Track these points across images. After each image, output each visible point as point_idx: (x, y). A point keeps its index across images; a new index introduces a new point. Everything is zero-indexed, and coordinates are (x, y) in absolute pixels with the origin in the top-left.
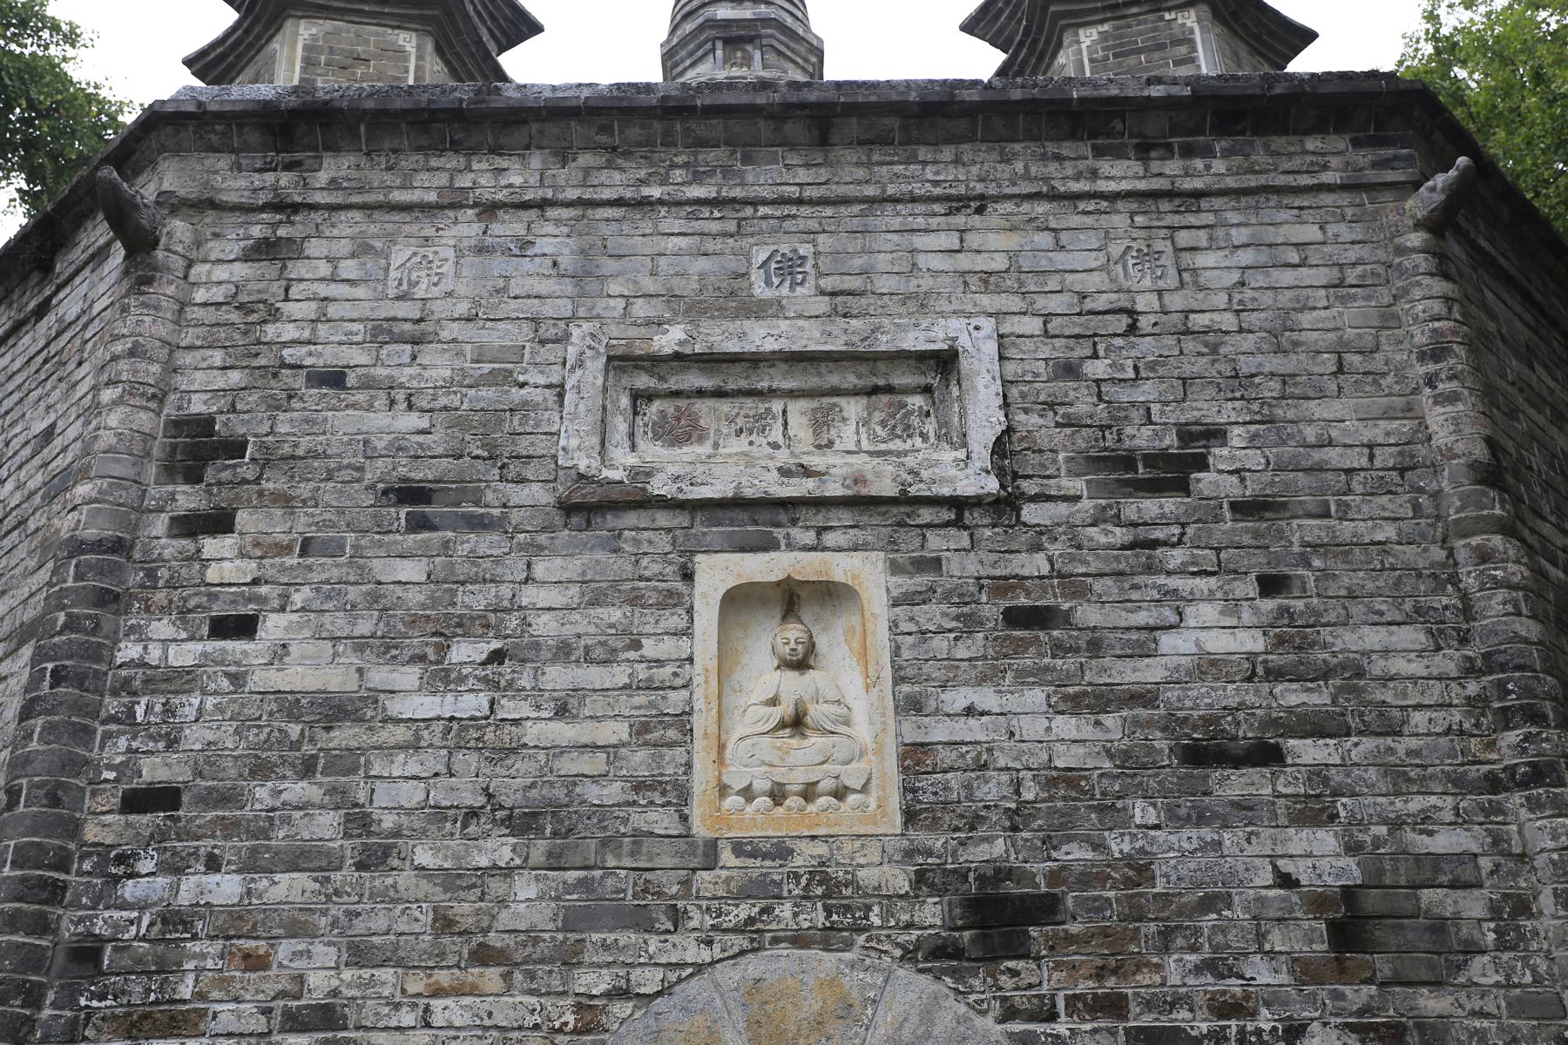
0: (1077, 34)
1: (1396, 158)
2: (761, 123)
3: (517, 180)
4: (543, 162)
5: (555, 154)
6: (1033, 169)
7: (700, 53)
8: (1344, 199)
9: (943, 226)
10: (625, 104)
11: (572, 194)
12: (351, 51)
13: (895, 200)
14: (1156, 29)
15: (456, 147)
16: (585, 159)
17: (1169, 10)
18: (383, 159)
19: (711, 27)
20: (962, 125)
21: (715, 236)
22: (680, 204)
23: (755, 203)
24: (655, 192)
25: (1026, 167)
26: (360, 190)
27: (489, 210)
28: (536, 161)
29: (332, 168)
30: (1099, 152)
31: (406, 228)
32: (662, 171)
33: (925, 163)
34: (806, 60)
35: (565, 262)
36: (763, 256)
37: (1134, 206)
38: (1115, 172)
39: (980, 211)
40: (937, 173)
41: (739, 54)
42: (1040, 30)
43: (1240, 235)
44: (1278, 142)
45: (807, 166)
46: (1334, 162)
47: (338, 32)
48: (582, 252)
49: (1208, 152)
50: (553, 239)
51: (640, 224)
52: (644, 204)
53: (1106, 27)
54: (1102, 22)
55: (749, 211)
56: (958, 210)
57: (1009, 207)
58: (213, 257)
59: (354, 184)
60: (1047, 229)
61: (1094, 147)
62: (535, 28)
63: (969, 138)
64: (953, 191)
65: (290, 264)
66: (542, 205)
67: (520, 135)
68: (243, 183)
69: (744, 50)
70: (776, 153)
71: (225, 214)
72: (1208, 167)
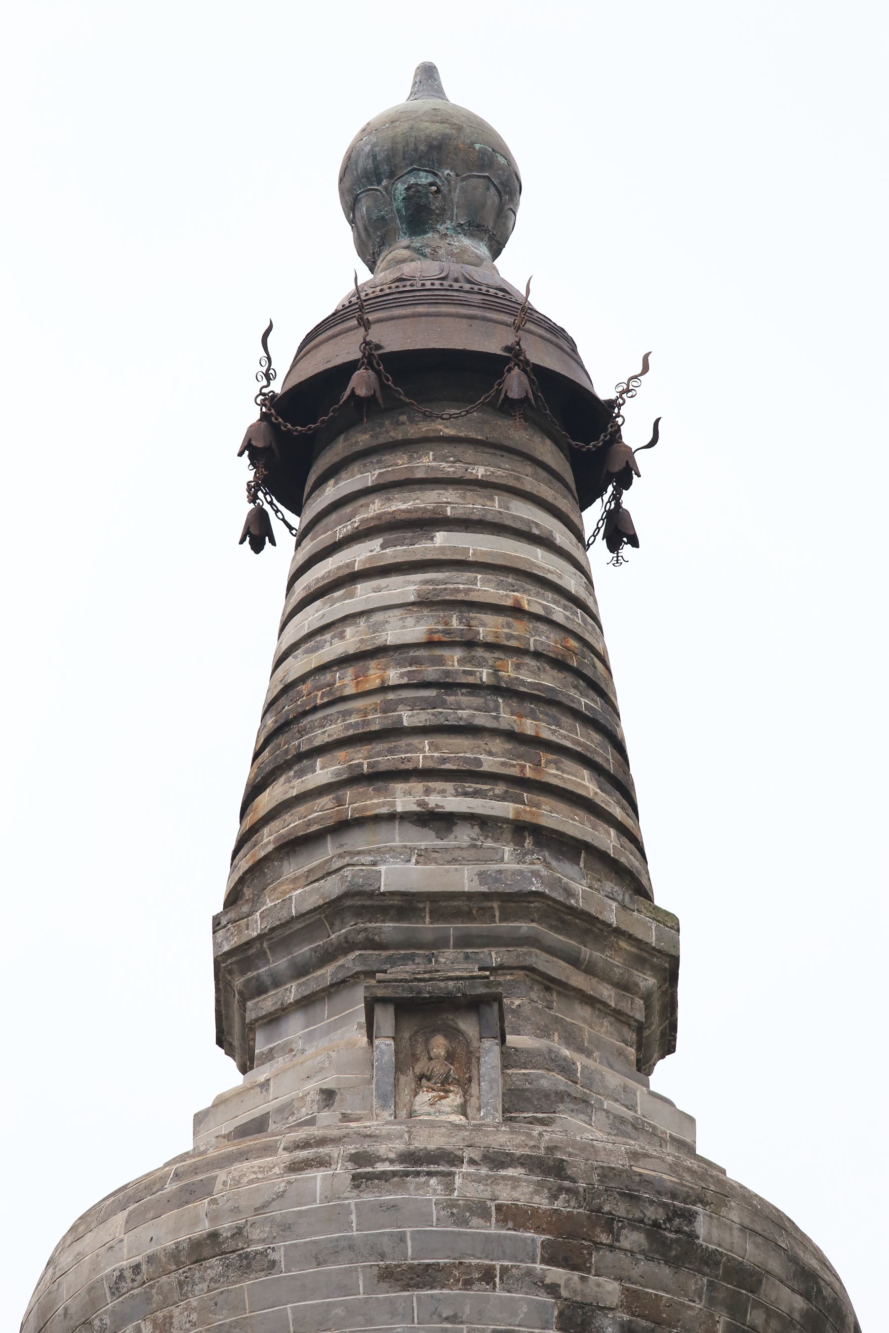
7: (327, 974)
19: (360, 912)
34: (625, 987)
41: (439, 1045)
69: (453, 1033)
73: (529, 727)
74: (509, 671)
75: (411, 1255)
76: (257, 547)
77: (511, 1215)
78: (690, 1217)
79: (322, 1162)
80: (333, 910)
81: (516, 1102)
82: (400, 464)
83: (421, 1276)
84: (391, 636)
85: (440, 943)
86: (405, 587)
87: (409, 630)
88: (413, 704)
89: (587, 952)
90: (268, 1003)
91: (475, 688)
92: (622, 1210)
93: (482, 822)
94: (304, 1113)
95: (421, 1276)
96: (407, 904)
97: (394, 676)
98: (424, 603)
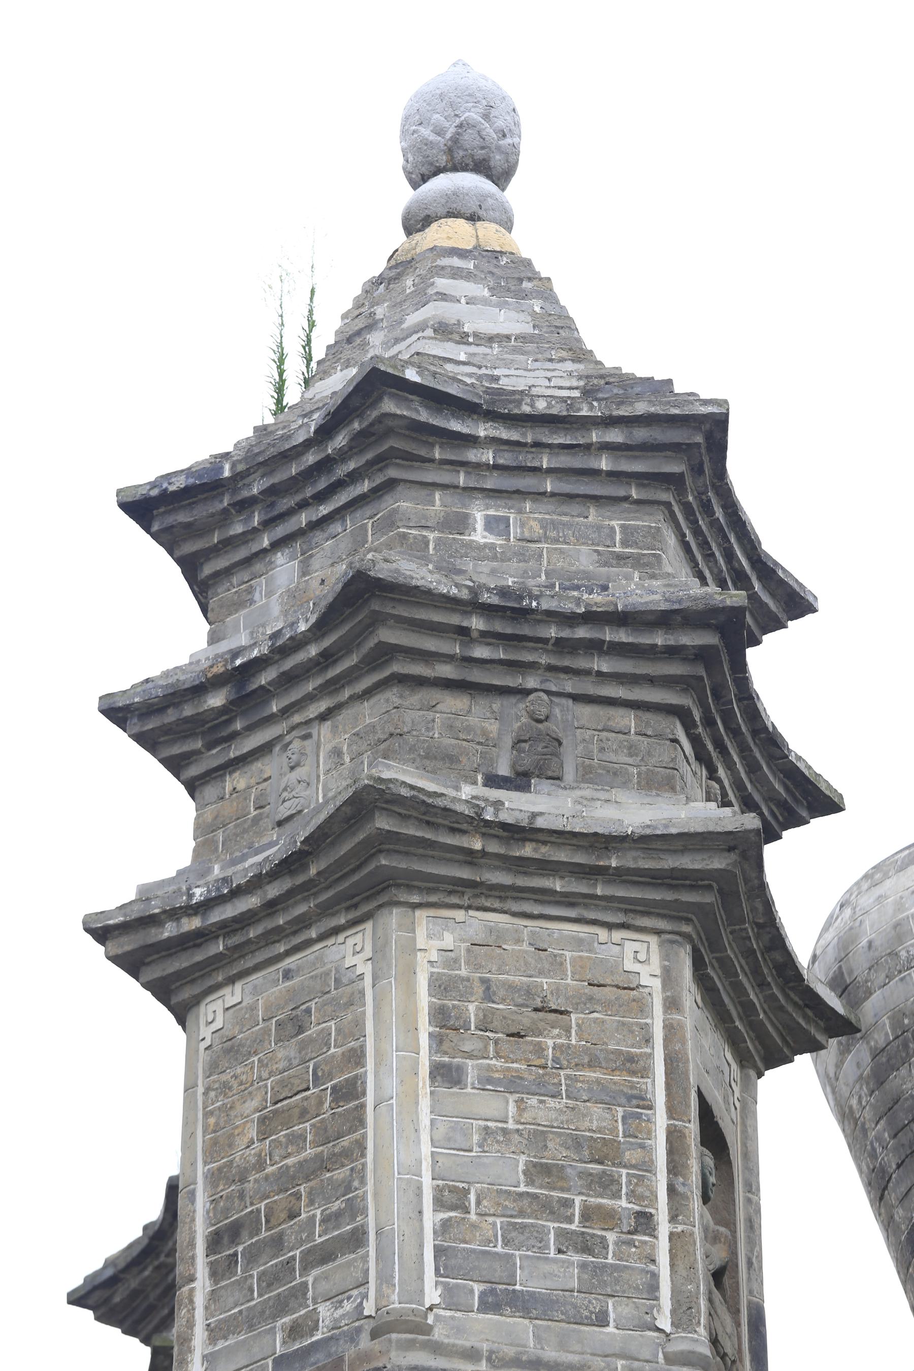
12: (529, 992)
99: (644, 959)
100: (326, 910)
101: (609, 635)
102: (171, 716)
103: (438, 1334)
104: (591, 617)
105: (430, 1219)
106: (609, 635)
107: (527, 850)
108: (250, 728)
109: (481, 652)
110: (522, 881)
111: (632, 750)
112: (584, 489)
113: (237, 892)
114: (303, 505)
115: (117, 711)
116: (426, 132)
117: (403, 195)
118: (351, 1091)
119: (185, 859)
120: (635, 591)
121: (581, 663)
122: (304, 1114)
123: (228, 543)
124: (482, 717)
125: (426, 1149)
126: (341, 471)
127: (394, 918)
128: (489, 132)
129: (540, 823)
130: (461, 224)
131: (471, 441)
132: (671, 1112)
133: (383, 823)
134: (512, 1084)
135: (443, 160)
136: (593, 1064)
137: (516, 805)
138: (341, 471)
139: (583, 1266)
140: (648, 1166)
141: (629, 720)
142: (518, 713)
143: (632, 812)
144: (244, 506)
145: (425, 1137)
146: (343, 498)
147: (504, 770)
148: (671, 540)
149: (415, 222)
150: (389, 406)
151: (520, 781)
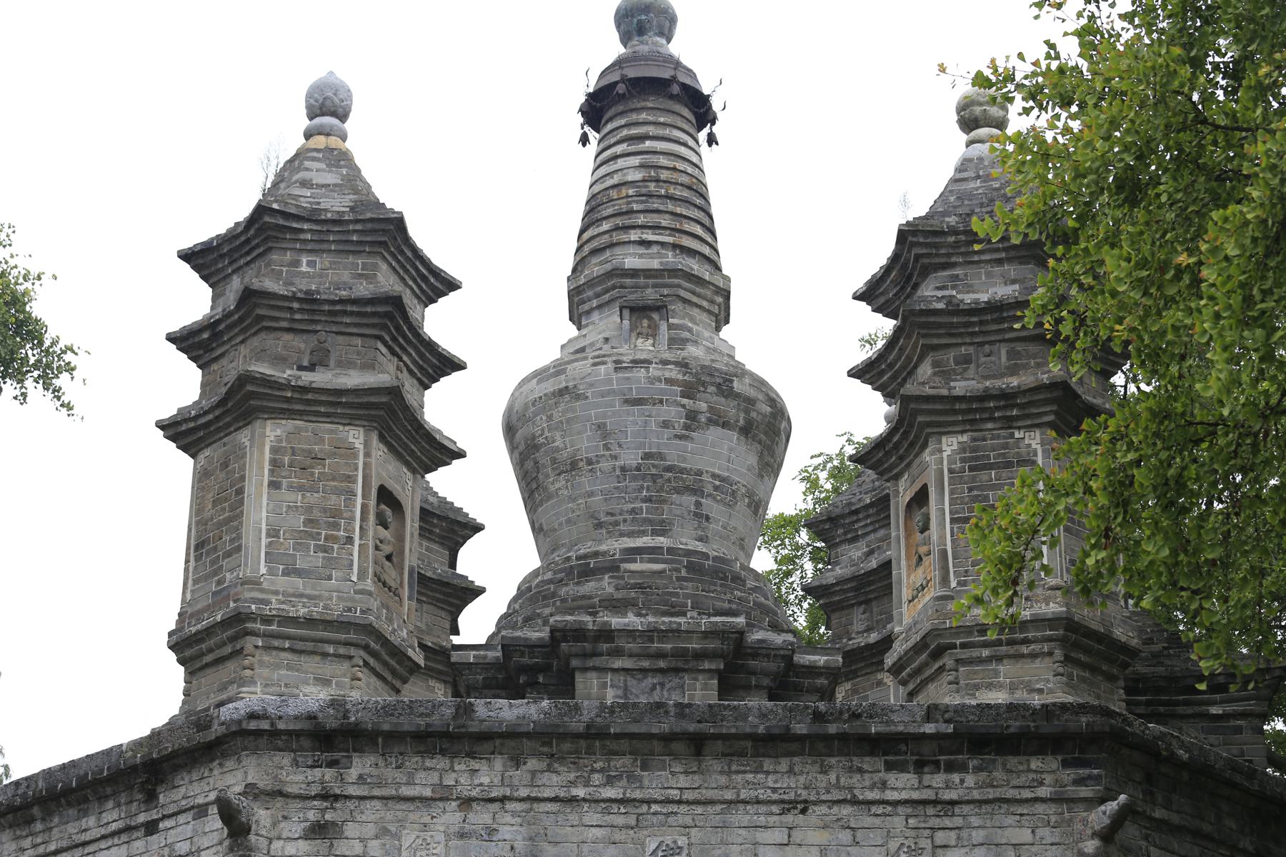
0: (940, 442)
1: (1090, 777)
2: (655, 743)
3: (486, 780)
4: (504, 766)
5: (512, 759)
6: (842, 780)
7: (607, 297)
8: (1051, 809)
9: (778, 824)
10: (561, 730)
11: (523, 792)
12: (310, 451)
13: (745, 802)
14: (1005, 446)
15: (443, 752)
16: (532, 764)
17: (1019, 428)
18: (393, 760)
20: (795, 746)
21: (621, 828)
22: (597, 801)
23: (649, 802)
24: (580, 792)
25: (838, 778)
26: (379, 785)
27: (466, 803)
28: (498, 763)
29: (361, 765)
30: (890, 767)
31: (411, 816)
32: (586, 775)
33: (768, 773)
34: (712, 302)
35: (519, 845)
36: (653, 846)
37: (909, 810)
38: (899, 784)
39: (804, 811)
40: (776, 782)
41: (645, 323)
42: (911, 426)
43: (978, 836)
44: (1012, 761)
45: (686, 773)
46: (1048, 779)
47: (298, 431)
48: (531, 839)
49: (963, 768)
50: (511, 828)
51: (571, 817)
52: (573, 800)
53: (965, 438)
54: (962, 432)
55: (644, 808)
56: (789, 810)
57: (823, 809)
58: (284, 836)
59: (374, 780)
60: (848, 827)
61: (886, 762)
62: (452, 285)
63: (800, 753)
64: (786, 797)
65: (335, 842)
66: (503, 800)
67: (488, 746)
68: (300, 778)
69: (650, 318)
70: (664, 761)
71: (289, 800)
72: (962, 781)
73: (678, 210)
74: (671, 191)
75: (634, 395)
76: (584, 145)
77: (669, 381)
78: (732, 381)
79: (604, 363)
80: (609, 275)
81: (672, 341)
82: (634, 117)
83: (639, 402)
84: (630, 178)
85: (647, 286)
86: (635, 161)
87: (637, 176)
88: (637, 202)
89: (698, 290)
90: (586, 307)
91: (660, 197)
92: (708, 379)
93: (662, 244)
94: (598, 346)
95: (639, 402)
96: (634, 273)
97: (631, 192)
98: (642, 166)
99: (356, 437)
100: (236, 420)
101: (349, 308)
102: (191, 341)
103: (265, 585)
104: (341, 301)
105: (264, 541)
106: (349, 308)
107: (310, 396)
108: (218, 346)
109: (298, 316)
110: (308, 408)
111: (358, 353)
112: (348, 248)
113: (206, 413)
114: (241, 256)
115: (171, 338)
116: (312, 101)
117: (305, 123)
118: (240, 492)
119: (197, 398)
120: (363, 289)
121: (339, 319)
122: (226, 500)
123: (218, 271)
124: (298, 342)
125: (264, 514)
126: (254, 243)
127: (258, 423)
128: (336, 100)
129: (314, 385)
130: (322, 138)
131: (302, 231)
132: (364, 497)
133: (250, 388)
134: (301, 488)
135: (318, 112)
136: (333, 479)
137: (307, 378)
138: (254, 243)
139: (324, 558)
140: (353, 518)
141: (359, 341)
142: (313, 340)
143: (353, 379)
144: (222, 256)
145: (264, 510)
146: (255, 254)
147: (305, 363)
148: (384, 267)
149: (308, 135)
150: (267, 219)
151: (311, 368)
